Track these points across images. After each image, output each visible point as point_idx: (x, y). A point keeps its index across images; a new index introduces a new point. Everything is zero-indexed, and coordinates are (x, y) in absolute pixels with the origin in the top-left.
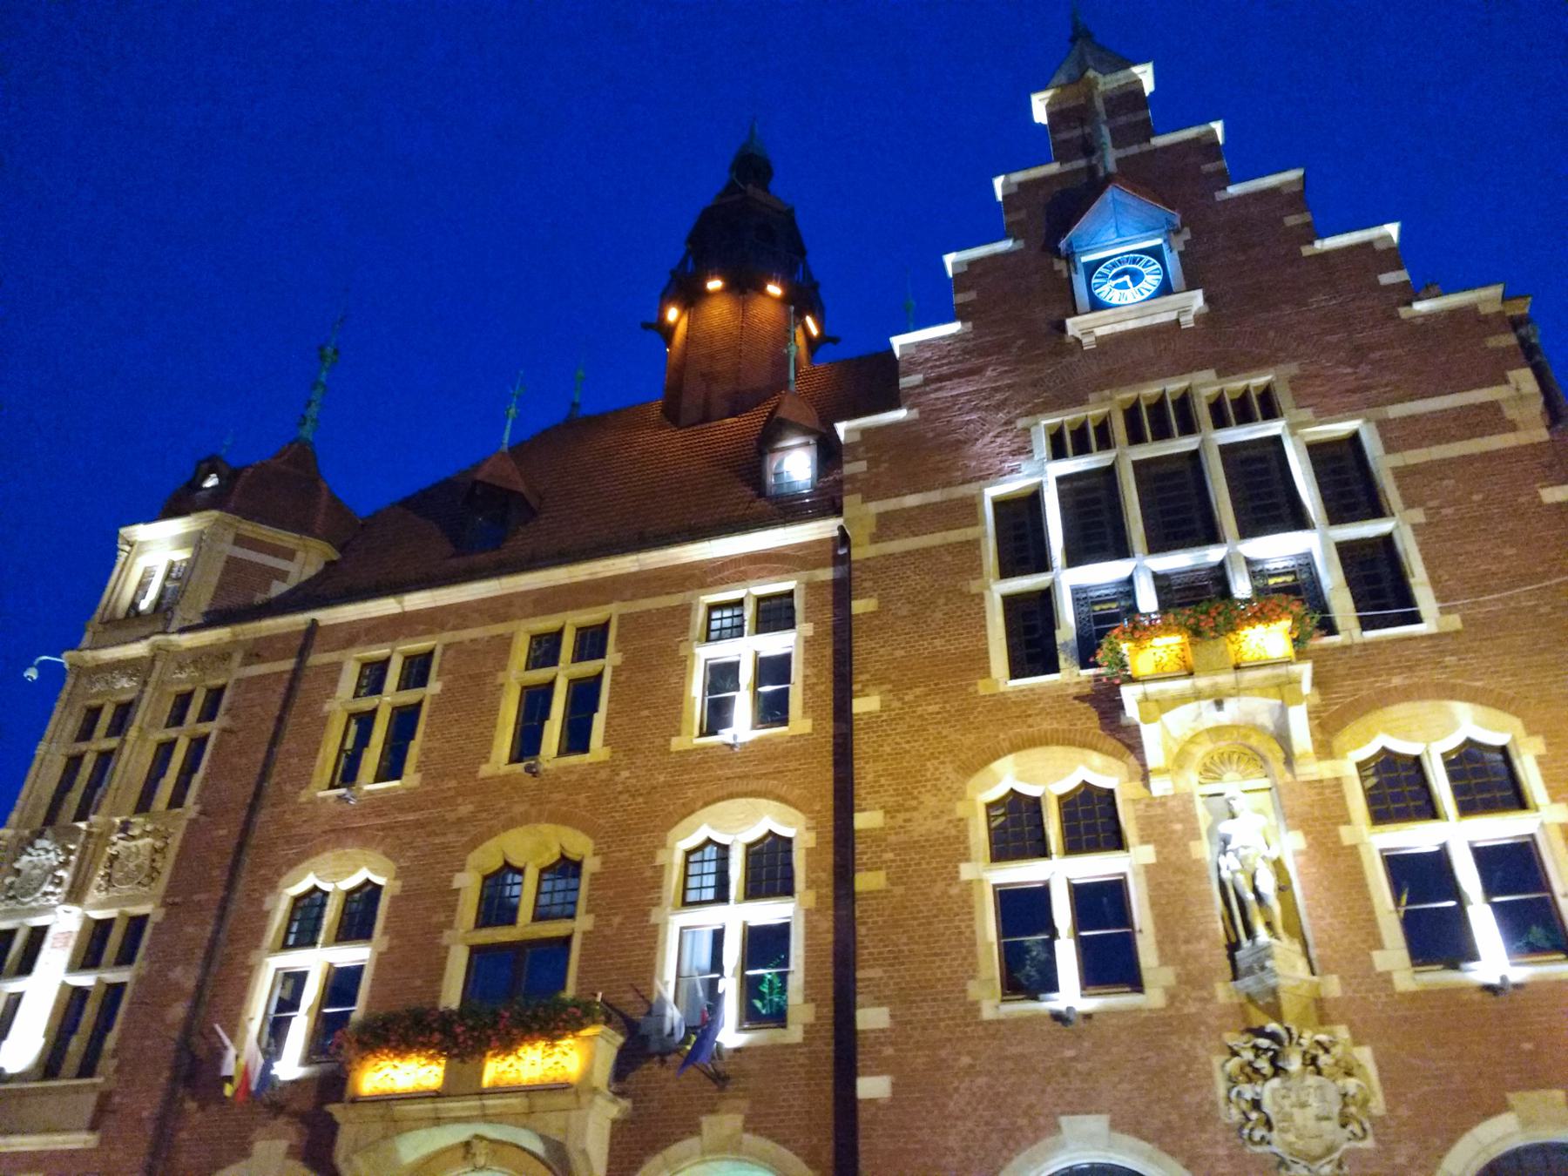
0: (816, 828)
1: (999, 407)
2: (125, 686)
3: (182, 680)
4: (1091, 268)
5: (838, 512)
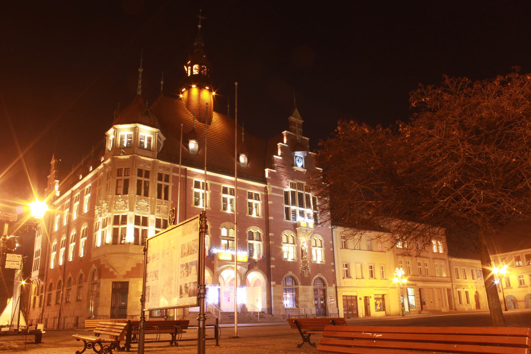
0: (263, 232)
1: (285, 176)
2: (148, 168)
3: (161, 171)
4: (296, 156)
5: (266, 184)
